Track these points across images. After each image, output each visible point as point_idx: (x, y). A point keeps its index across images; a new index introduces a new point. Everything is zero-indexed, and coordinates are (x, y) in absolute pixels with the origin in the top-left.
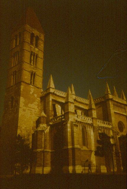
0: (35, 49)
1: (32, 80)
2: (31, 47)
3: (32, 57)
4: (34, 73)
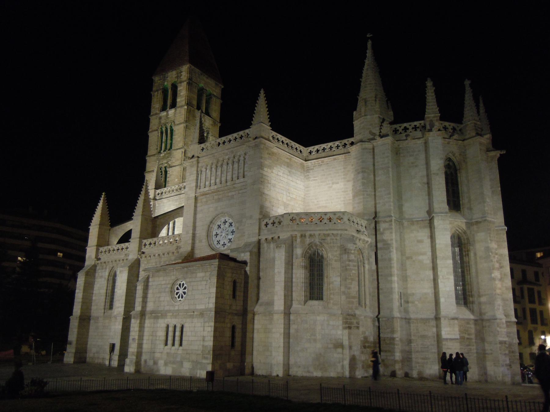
3: (164, 134)
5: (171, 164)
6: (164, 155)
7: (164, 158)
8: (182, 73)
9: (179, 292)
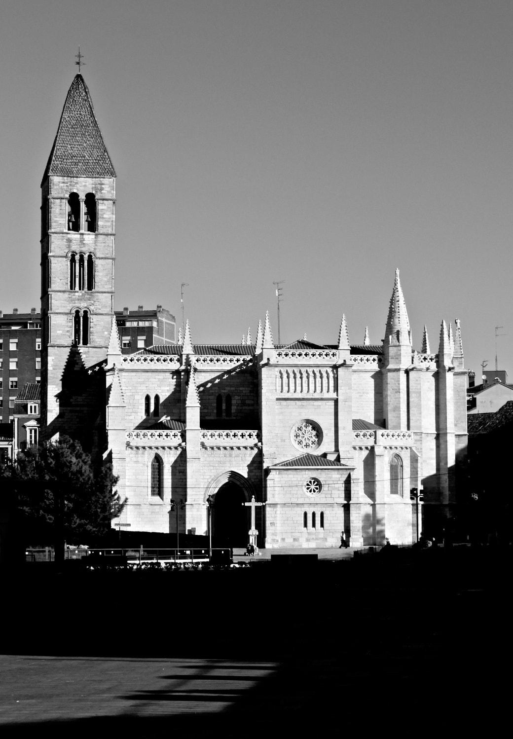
0: (82, 241)
2: (69, 241)
5: (95, 310)
6: (81, 294)
8: (103, 186)
9: (315, 488)
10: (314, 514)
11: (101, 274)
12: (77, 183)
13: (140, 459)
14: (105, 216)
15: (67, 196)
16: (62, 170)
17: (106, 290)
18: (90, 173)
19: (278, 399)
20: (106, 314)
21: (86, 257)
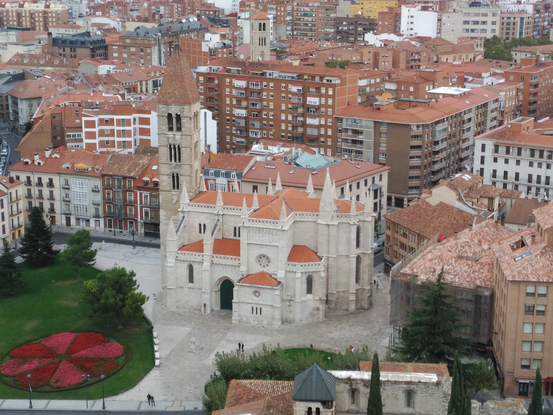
0: (174, 138)
1: (176, 184)
2: (168, 138)
4: (175, 175)
7: (175, 167)
10: (257, 308)
11: (184, 155)
12: (171, 108)
13: (183, 265)
14: (186, 125)
15: (166, 115)
16: (163, 102)
17: (187, 164)
18: (178, 103)
19: (248, 243)
20: (187, 176)
21: (177, 146)
